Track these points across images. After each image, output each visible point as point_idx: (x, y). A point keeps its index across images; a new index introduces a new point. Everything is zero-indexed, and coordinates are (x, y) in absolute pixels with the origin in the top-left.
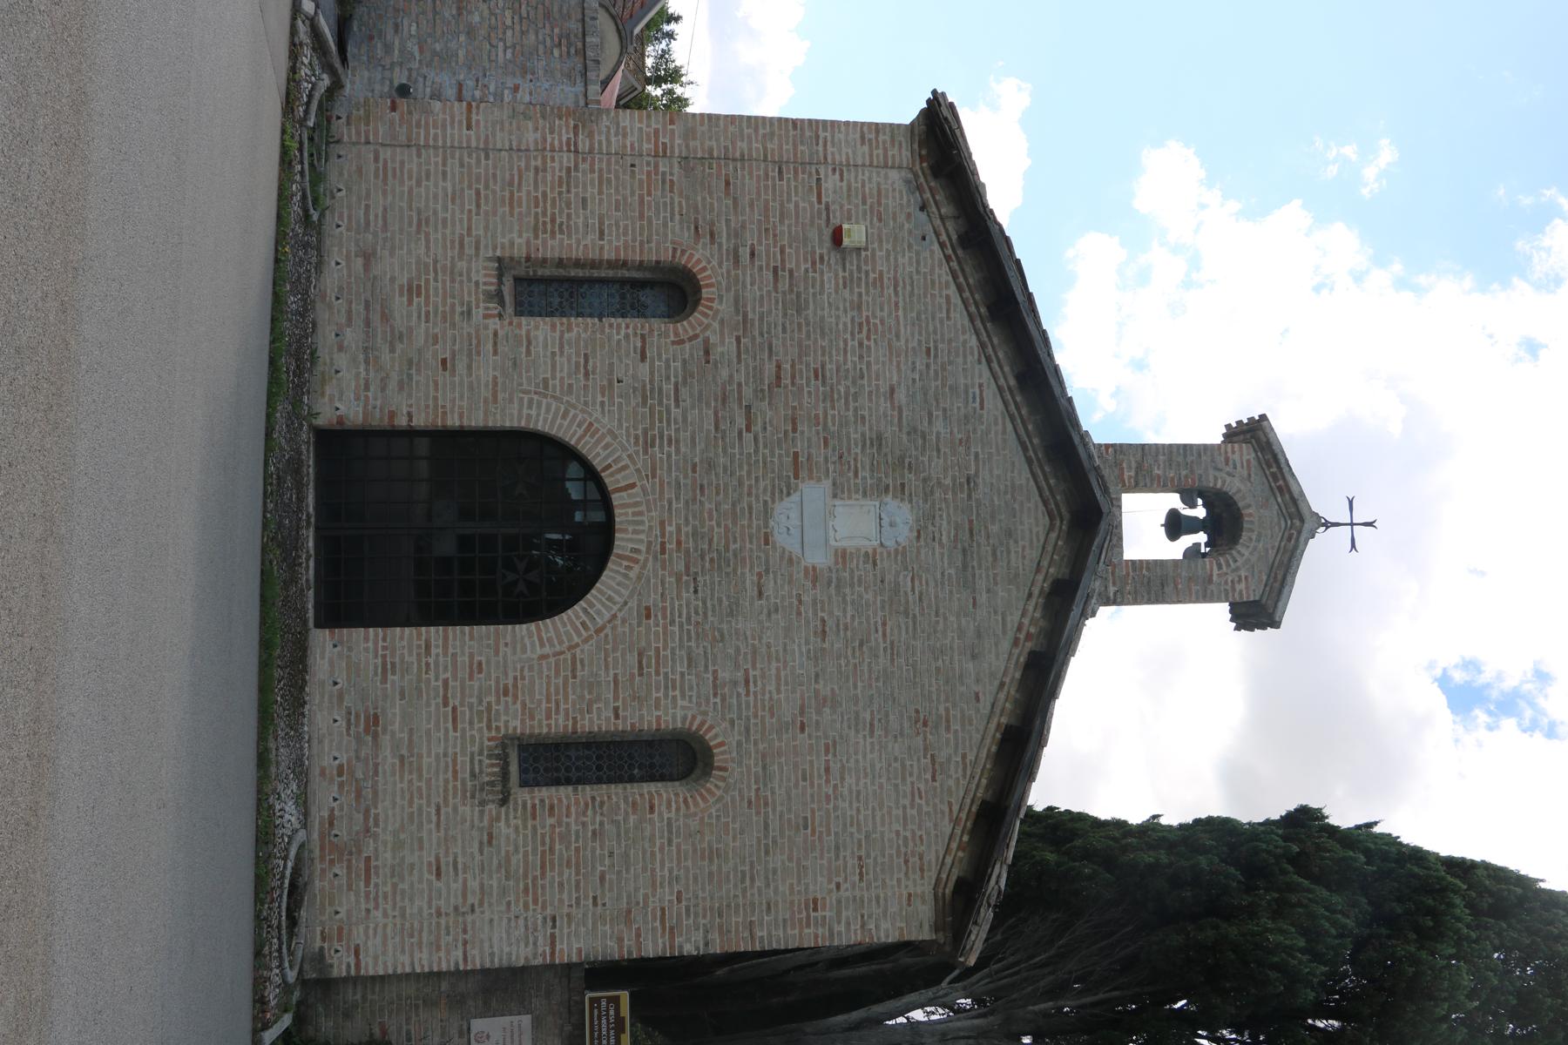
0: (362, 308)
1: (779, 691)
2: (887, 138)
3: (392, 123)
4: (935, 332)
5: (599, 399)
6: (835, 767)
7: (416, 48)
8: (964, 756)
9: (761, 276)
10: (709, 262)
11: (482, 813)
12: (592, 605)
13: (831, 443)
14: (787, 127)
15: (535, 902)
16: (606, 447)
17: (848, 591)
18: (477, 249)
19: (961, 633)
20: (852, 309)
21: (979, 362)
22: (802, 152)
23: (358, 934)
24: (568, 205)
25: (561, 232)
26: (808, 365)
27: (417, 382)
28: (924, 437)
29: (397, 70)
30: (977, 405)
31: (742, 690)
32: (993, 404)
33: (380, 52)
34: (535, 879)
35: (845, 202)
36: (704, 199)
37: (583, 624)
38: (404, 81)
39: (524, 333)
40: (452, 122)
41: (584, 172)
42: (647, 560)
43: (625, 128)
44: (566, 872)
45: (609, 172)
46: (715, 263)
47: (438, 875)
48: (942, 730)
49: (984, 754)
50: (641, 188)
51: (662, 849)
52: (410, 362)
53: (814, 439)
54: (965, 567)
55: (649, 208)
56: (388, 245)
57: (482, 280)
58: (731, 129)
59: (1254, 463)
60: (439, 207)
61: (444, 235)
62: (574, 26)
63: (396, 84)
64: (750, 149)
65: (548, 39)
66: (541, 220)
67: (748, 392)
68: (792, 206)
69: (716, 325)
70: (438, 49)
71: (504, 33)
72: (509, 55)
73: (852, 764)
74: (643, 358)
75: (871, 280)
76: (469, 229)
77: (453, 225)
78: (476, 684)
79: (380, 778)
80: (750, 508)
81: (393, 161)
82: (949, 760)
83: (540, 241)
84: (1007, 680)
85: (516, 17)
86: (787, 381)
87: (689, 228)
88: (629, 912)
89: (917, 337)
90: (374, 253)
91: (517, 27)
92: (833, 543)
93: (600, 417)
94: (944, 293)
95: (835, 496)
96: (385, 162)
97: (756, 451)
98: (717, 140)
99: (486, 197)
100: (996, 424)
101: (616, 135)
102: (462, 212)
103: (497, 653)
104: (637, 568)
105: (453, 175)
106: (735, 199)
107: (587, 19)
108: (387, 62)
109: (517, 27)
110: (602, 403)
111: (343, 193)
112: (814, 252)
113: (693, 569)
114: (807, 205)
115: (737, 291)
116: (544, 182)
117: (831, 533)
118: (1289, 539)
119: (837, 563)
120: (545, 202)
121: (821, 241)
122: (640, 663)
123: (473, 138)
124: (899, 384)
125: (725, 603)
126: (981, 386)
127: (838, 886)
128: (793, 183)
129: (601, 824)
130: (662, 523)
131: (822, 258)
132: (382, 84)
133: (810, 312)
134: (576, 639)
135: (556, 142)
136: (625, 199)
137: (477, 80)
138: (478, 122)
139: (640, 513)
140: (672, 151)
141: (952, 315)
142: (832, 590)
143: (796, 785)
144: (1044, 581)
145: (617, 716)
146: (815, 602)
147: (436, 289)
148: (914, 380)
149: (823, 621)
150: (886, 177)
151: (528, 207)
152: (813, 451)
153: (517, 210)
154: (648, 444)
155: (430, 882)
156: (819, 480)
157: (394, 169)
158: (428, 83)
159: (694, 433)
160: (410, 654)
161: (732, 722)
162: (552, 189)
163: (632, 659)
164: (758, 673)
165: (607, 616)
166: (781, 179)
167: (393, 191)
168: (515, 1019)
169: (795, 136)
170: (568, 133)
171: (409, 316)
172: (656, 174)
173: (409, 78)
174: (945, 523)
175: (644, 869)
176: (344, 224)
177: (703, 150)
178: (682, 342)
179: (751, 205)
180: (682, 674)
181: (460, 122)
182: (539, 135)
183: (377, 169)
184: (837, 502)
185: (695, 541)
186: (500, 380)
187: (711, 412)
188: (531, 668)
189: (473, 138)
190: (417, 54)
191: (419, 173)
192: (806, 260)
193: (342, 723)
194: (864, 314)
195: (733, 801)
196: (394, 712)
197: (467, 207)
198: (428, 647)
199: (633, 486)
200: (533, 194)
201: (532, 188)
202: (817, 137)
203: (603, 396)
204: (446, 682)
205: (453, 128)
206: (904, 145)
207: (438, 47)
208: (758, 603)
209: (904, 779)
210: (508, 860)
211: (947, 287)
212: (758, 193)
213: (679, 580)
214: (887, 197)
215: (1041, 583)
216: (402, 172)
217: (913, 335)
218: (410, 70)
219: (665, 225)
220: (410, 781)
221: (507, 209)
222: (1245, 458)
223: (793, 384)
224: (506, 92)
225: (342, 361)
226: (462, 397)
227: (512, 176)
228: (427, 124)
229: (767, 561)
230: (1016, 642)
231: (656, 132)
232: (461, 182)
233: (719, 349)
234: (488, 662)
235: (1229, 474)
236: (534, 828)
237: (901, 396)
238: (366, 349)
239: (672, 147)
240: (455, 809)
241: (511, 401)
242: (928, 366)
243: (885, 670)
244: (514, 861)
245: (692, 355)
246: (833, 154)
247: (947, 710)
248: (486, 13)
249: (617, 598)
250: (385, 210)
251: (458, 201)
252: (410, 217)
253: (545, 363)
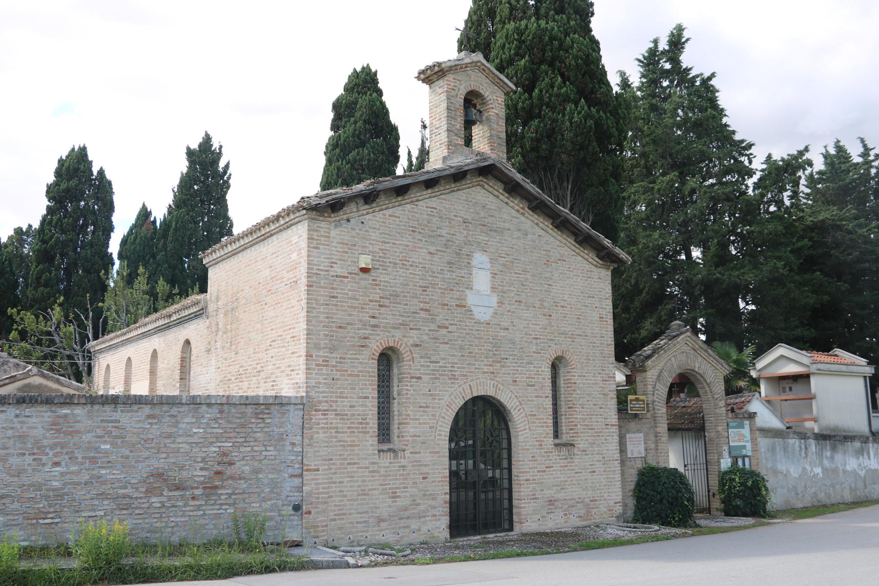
0: (402, 521)
1: (539, 325)
2: (315, 234)
3: (318, 513)
4: (405, 226)
5: (437, 401)
6: (562, 303)
7: (269, 503)
8: (558, 246)
9: (383, 314)
10: (378, 341)
11: (577, 455)
12: (512, 407)
13: (452, 288)
14: (312, 291)
15: (601, 432)
16: (455, 398)
17: (505, 288)
18: (374, 463)
19: (518, 238)
20: (396, 268)
21: (417, 205)
22: (324, 284)
23: (612, 503)
24: (354, 415)
25: (365, 419)
26: (421, 295)
27: (432, 491)
28: (448, 241)
29: (283, 513)
30: (435, 211)
31: (539, 341)
32: (434, 202)
33: (272, 523)
34: (595, 432)
35: (347, 263)
36: (348, 341)
37: (519, 411)
38: (291, 508)
39: (411, 439)
40: (315, 479)
41: (337, 406)
42: (497, 381)
43: (316, 383)
44: (593, 420)
45: (336, 392)
46: (378, 338)
47: (594, 472)
48: (550, 254)
49: (559, 238)
50: (344, 375)
51: (587, 380)
52: (425, 495)
53: (450, 296)
54: (496, 231)
55: (354, 371)
56: (374, 510)
57: (389, 460)
58: (314, 322)
59: (454, 76)
60: (356, 484)
61: (370, 481)
62: (249, 410)
63: (293, 512)
64: (324, 313)
65: (259, 426)
66: (361, 430)
67: (433, 327)
68: (350, 293)
69: (405, 340)
70: (269, 490)
71: (256, 451)
72: (272, 448)
73: (560, 296)
74: (420, 378)
75: (383, 255)
76: (366, 468)
77: (364, 476)
78: (539, 458)
79: (568, 498)
80: (477, 330)
81: (335, 511)
82: (559, 253)
83: (370, 430)
84: (536, 221)
85: (245, 444)
86: (427, 306)
87: (362, 350)
88: (604, 394)
89: (407, 236)
90: (378, 517)
91: (252, 444)
93: (443, 401)
94: (387, 217)
96: (335, 515)
97: (456, 325)
98: (320, 331)
99: (350, 459)
100: (442, 203)
101: (319, 388)
102: (358, 472)
103: (528, 449)
104: (499, 386)
105: (341, 477)
106: (348, 324)
107: (247, 402)
108: (278, 519)
109: (252, 444)
110: (439, 399)
111: (351, 536)
112: (371, 284)
113: (499, 360)
114: (349, 285)
115: (390, 327)
116: (342, 428)
117: (485, 293)
118: (484, 70)
119: (495, 292)
120: (353, 428)
121: (365, 280)
122: (531, 386)
123: (323, 467)
124: (427, 249)
125: (510, 345)
126: (427, 207)
127: (596, 307)
128: (339, 291)
129: (580, 405)
130: (484, 373)
131: (374, 280)
132: (293, 520)
133: (398, 290)
134: (524, 414)
135: (324, 421)
136: (349, 384)
137: (288, 466)
138: (315, 465)
139: (480, 383)
140: (327, 357)
141: (397, 215)
142: (505, 295)
143: (568, 321)
144: (503, 195)
145: (548, 397)
146: (510, 304)
147: (393, 484)
148: (426, 241)
149: (516, 301)
150: (334, 238)
151: (355, 436)
152: (455, 297)
153: (357, 443)
154: (454, 378)
155: (597, 475)
156: (466, 295)
157: (339, 510)
158: (291, 494)
159: (449, 355)
160: (529, 488)
161: (549, 346)
162: (346, 424)
163: (530, 389)
164: (533, 333)
165: (516, 400)
166: (337, 297)
167: (350, 509)
168: (628, 440)
169: (316, 287)
170: (319, 415)
171: (405, 497)
172: (337, 366)
173: (289, 505)
174: (480, 237)
175: (592, 387)
176: (365, 534)
177: (326, 339)
178: (413, 358)
179: (350, 315)
180: (534, 367)
181: (315, 475)
182: (320, 431)
183: (339, 519)
184: (474, 287)
185: (490, 357)
186: (431, 450)
187: (441, 345)
188: (533, 434)
189: (323, 467)
190: (273, 502)
191: (340, 496)
192: (375, 289)
193: (551, 515)
194: (398, 262)
195: (573, 349)
196: (549, 493)
197: (356, 470)
198: (527, 480)
199: (470, 385)
200: (348, 434)
201: (346, 435)
202: (316, 274)
203: (435, 399)
204: (539, 472)
205: (318, 479)
206: (319, 225)
207: (267, 490)
208: (510, 331)
209: (565, 274)
210: (589, 444)
211: (384, 215)
212: (345, 311)
213: (503, 366)
214: (343, 239)
215: (504, 197)
216: (340, 506)
217: (407, 238)
218: (283, 505)
219: (361, 363)
220: (569, 485)
221: (356, 448)
222: (451, 79)
223: (429, 303)
224: (295, 450)
225: (424, 529)
226: (437, 469)
227: (341, 446)
228: (318, 493)
229: (496, 324)
230: (523, 214)
231: (317, 365)
232: (344, 473)
233: (415, 339)
234: (531, 453)
235: (459, 91)
236: (581, 433)
237: (432, 249)
238: (420, 518)
239: (325, 357)
240: (576, 466)
241: (439, 445)
242: (420, 233)
243: (531, 276)
244: (590, 441)
245: (418, 353)
246: (324, 266)
247: (544, 250)
248: (244, 463)
249: (510, 395)
250: (358, 513)
251: (353, 475)
252: (362, 499)
253: (423, 428)
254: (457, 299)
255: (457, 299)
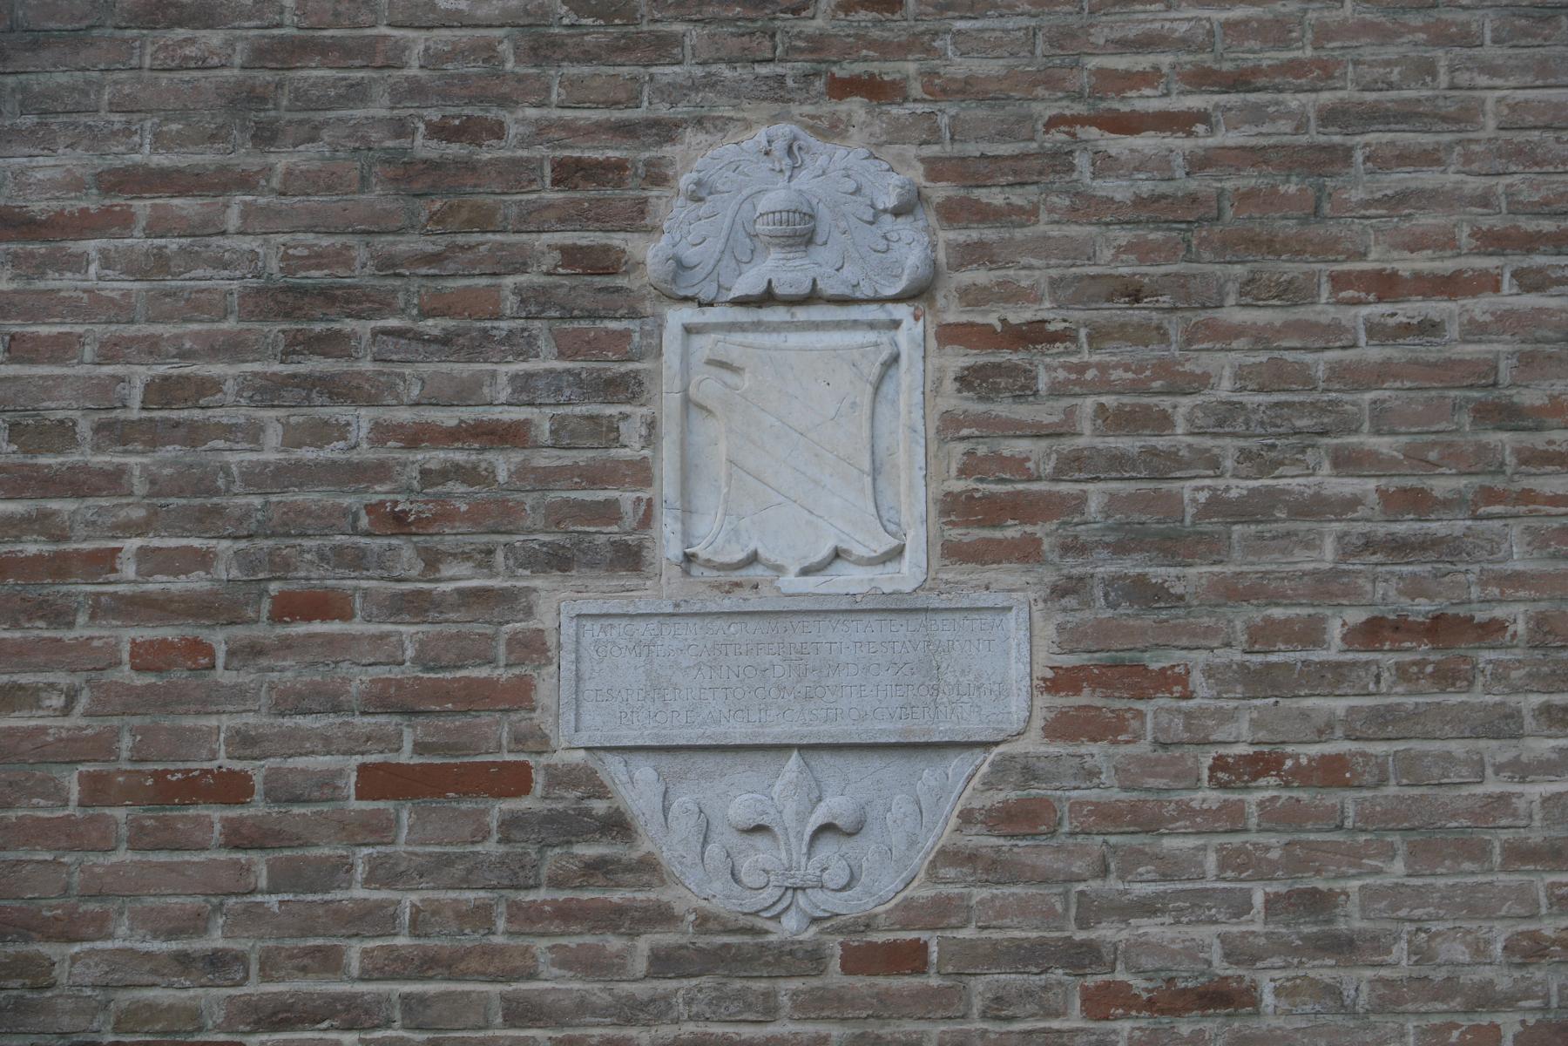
13: (312, 577)
17: (1191, 491)
53: (289, 673)
92: (907, 575)
95: (630, 558)
117: (850, 580)
119: (1027, 552)
146: (1261, 681)
149: (1372, 632)
152: (359, 680)
156: (533, 647)
184: (668, 541)
254: (382, 701)
255: (382, 701)
